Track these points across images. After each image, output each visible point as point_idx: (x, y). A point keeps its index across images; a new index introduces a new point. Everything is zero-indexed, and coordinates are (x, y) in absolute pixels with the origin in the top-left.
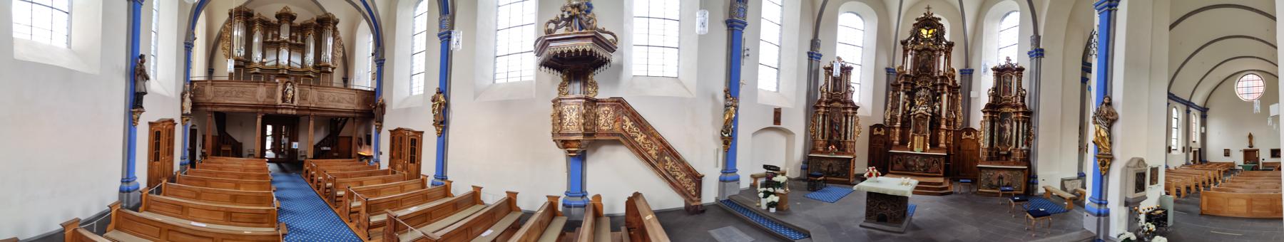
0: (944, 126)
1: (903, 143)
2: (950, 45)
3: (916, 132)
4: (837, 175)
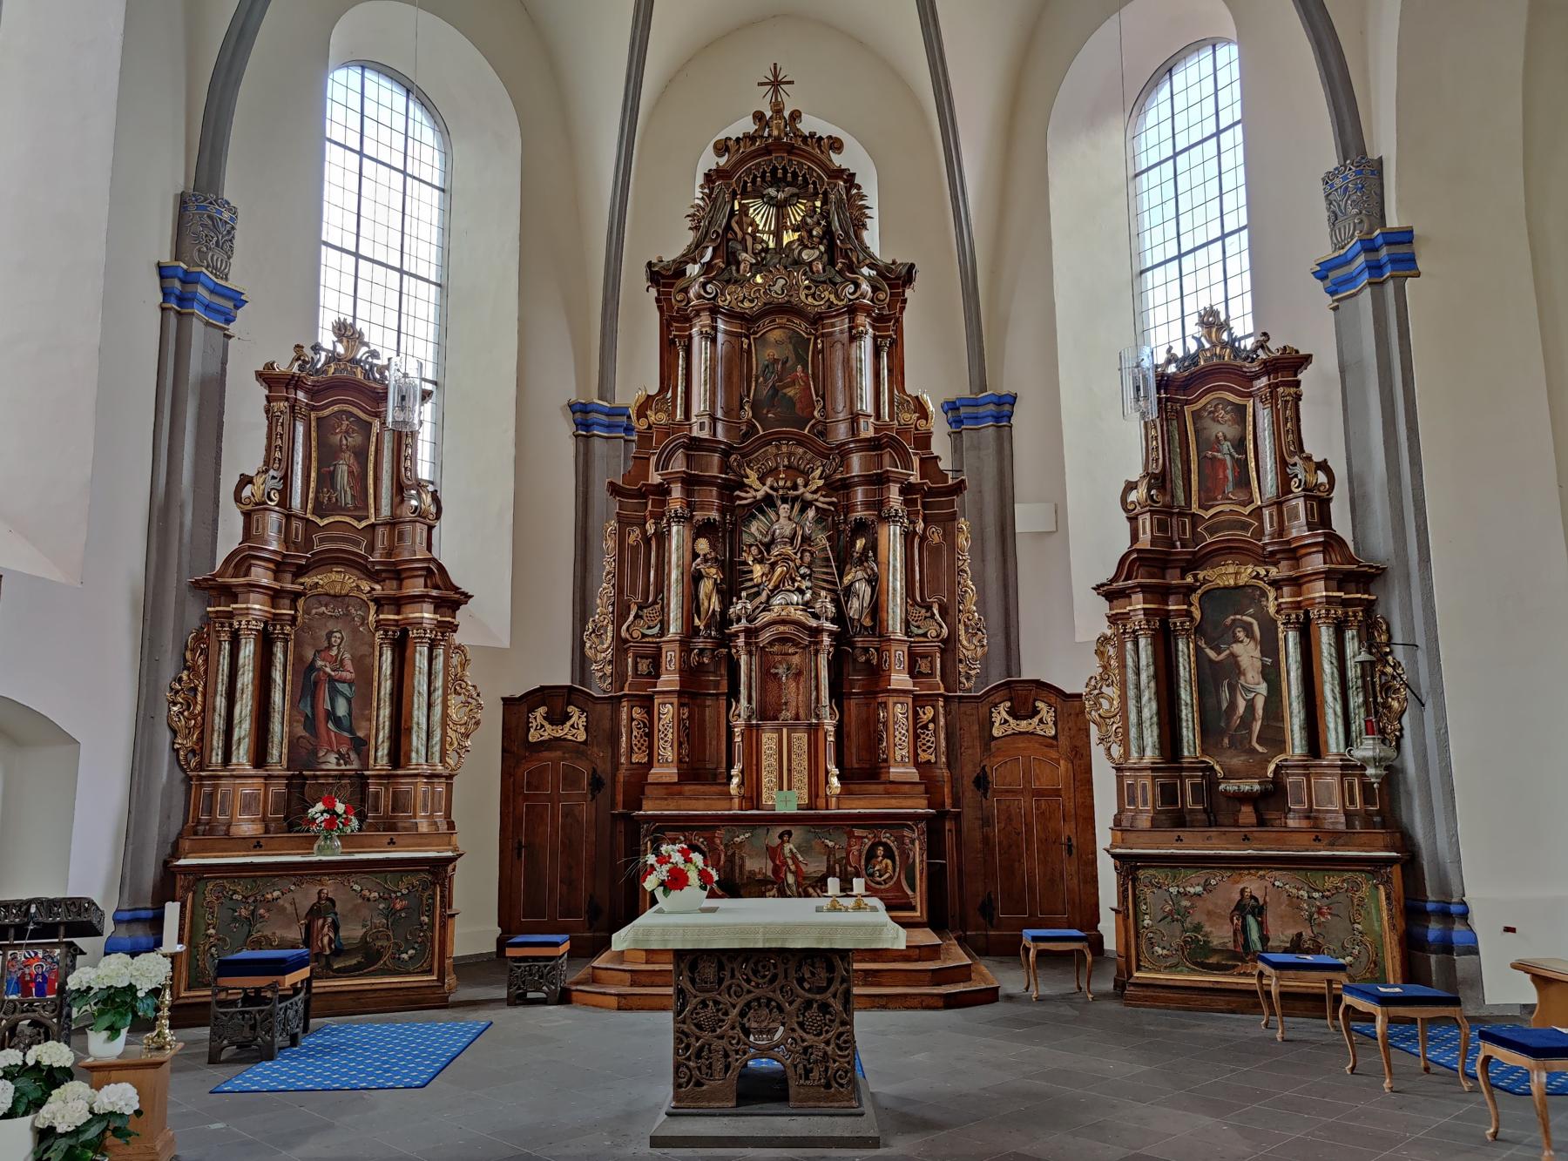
0: (900, 679)
1: (698, 770)
2: (897, 279)
3: (767, 712)
4: (368, 957)
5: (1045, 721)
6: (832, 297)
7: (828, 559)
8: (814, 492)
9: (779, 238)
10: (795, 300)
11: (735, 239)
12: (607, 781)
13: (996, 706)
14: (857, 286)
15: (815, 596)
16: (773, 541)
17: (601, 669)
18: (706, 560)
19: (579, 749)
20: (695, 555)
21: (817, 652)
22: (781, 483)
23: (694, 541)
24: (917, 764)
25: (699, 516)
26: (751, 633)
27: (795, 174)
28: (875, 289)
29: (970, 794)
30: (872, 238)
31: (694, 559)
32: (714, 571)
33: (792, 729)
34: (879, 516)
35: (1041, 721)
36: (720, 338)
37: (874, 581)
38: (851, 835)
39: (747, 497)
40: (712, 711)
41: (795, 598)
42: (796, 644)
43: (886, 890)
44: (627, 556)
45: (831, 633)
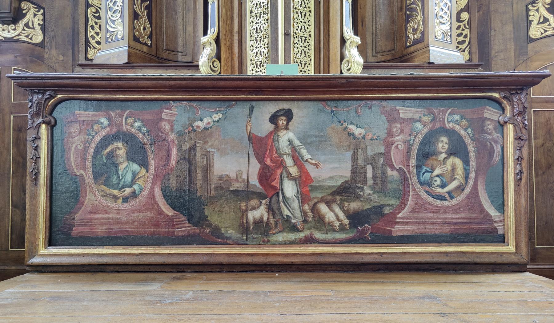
43: (454, 209)
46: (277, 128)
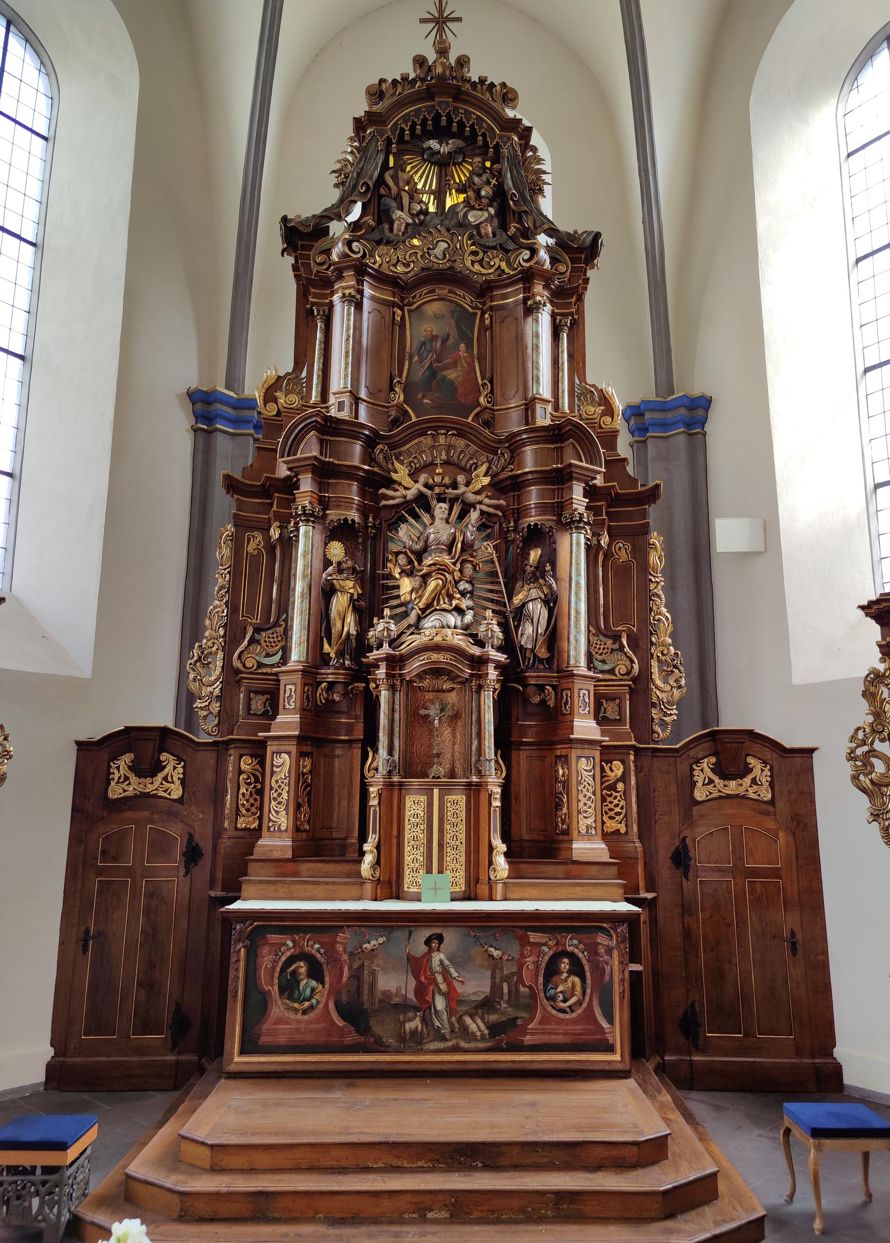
0: (585, 727)
1: (322, 844)
2: (581, 251)
5: (757, 782)
6: (503, 265)
7: (494, 574)
8: (477, 493)
9: (441, 203)
10: (459, 266)
11: (389, 196)
12: (207, 847)
13: (698, 761)
14: (534, 251)
15: (476, 621)
16: (425, 549)
17: (207, 708)
18: (340, 571)
19: (172, 810)
20: (327, 563)
21: (480, 688)
22: (438, 479)
23: (326, 544)
24: (606, 836)
25: (333, 515)
26: (395, 662)
27: (461, 124)
28: (554, 260)
29: (665, 870)
30: (546, 205)
31: (325, 569)
32: (350, 584)
33: (446, 790)
34: (559, 522)
35: (754, 781)
36: (366, 303)
37: (551, 602)
38: (524, 941)
39: (395, 497)
40: (344, 761)
41: (452, 619)
42: (453, 678)
43: (573, 1022)
44: (245, 567)
45: (498, 666)
46: (431, 950)
